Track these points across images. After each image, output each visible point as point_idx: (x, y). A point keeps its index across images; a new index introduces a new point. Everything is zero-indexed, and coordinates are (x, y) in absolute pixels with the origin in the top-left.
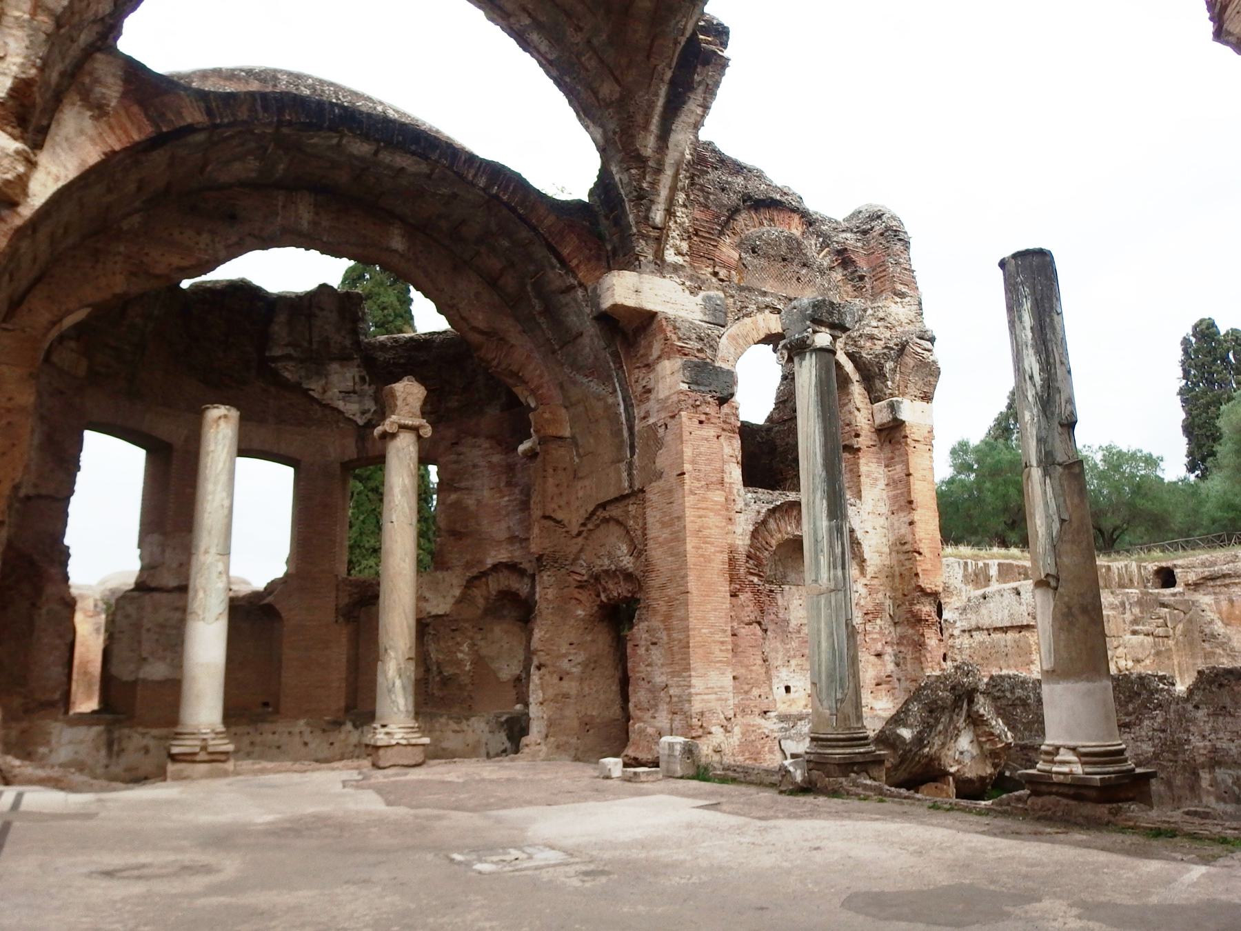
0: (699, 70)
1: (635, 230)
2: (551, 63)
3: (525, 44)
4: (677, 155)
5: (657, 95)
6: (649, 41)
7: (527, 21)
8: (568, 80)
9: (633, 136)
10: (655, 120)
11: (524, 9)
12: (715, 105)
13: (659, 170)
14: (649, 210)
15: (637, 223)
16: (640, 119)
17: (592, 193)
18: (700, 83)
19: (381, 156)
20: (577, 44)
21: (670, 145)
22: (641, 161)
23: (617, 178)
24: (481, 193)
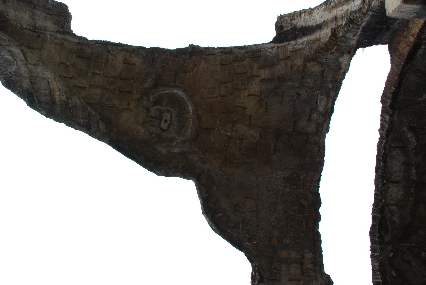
0: (286, 29)
1: (370, 13)
2: (328, 96)
3: (330, 111)
4: (326, 13)
5: (302, 44)
6: (281, 62)
7: (315, 116)
8: (330, 86)
9: (325, 44)
10: (314, 37)
11: (309, 119)
12: (298, 10)
13: (335, 19)
14: (355, 12)
15: (365, 14)
16: (315, 46)
17: (384, 44)
18: (292, 24)
19: (397, 179)
20: (306, 91)
21: (322, 21)
22: (334, 33)
23: (356, 38)
24: (395, 116)
